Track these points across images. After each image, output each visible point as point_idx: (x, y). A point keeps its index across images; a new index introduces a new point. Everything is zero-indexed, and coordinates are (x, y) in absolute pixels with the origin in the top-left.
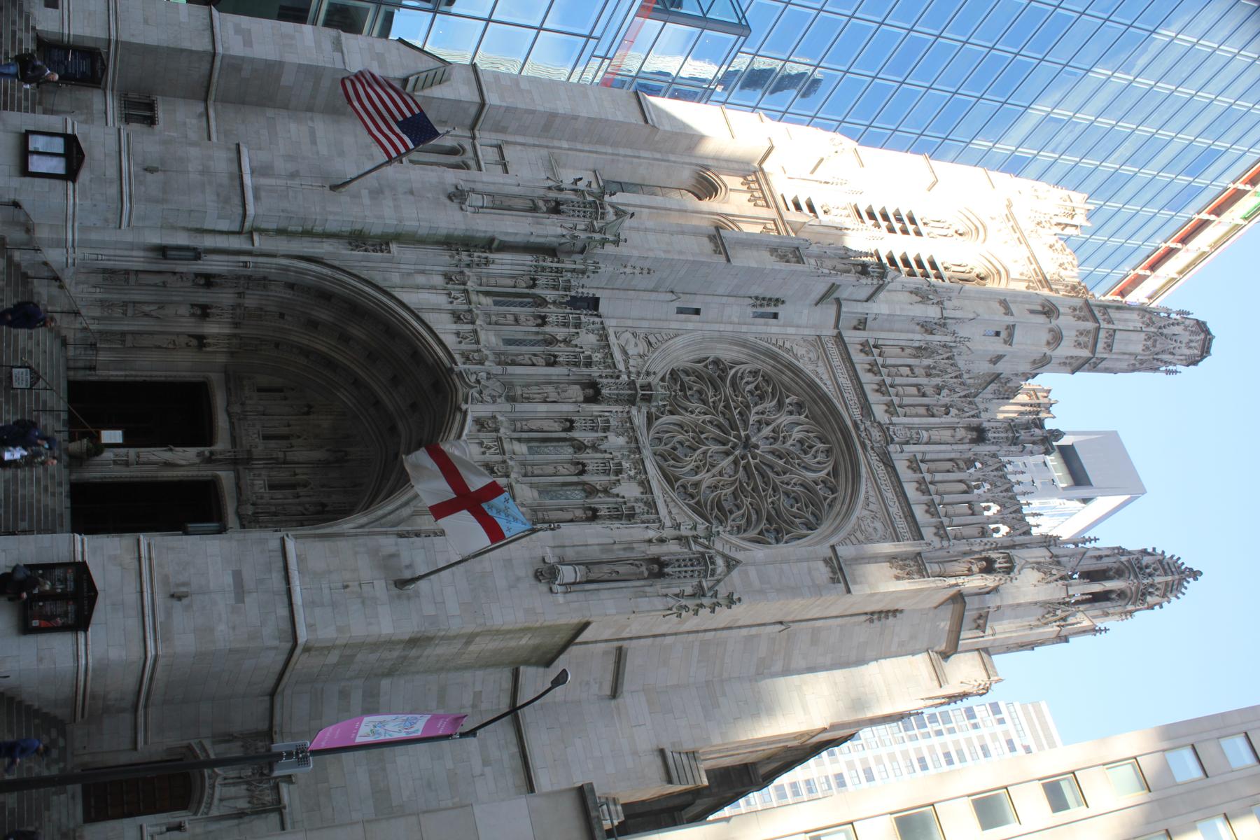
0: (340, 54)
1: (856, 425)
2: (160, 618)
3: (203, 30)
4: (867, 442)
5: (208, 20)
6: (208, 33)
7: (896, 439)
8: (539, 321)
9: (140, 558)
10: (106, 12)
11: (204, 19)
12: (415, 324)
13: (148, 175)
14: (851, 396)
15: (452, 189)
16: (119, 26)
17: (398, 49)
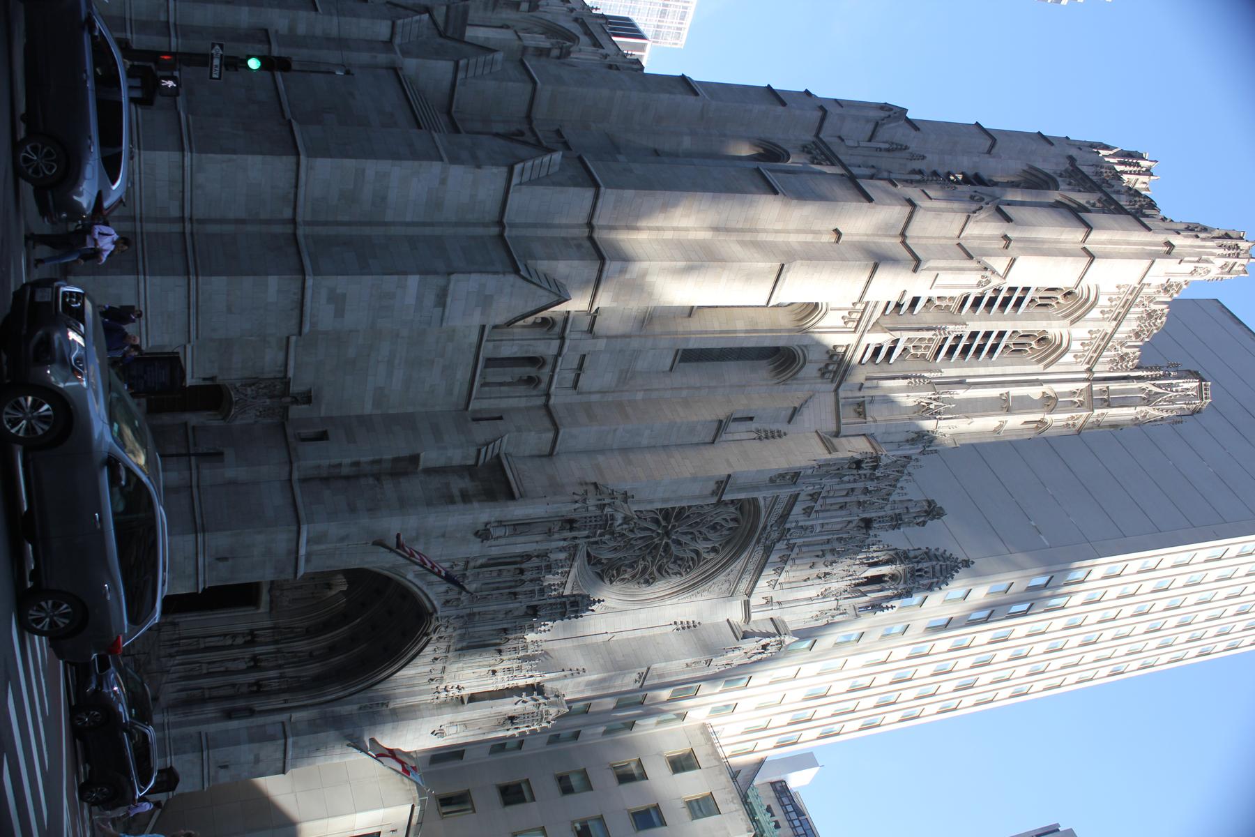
0: (441, 309)
1: (765, 528)
2: (212, 773)
3: (292, 310)
4: (763, 540)
5: (300, 296)
6: (296, 313)
7: (788, 537)
8: (518, 571)
9: (202, 759)
10: (187, 310)
11: (295, 294)
12: (416, 589)
13: (221, 564)
14: (779, 509)
15: (481, 527)
16: (200, 322)
17: (512, 286)
